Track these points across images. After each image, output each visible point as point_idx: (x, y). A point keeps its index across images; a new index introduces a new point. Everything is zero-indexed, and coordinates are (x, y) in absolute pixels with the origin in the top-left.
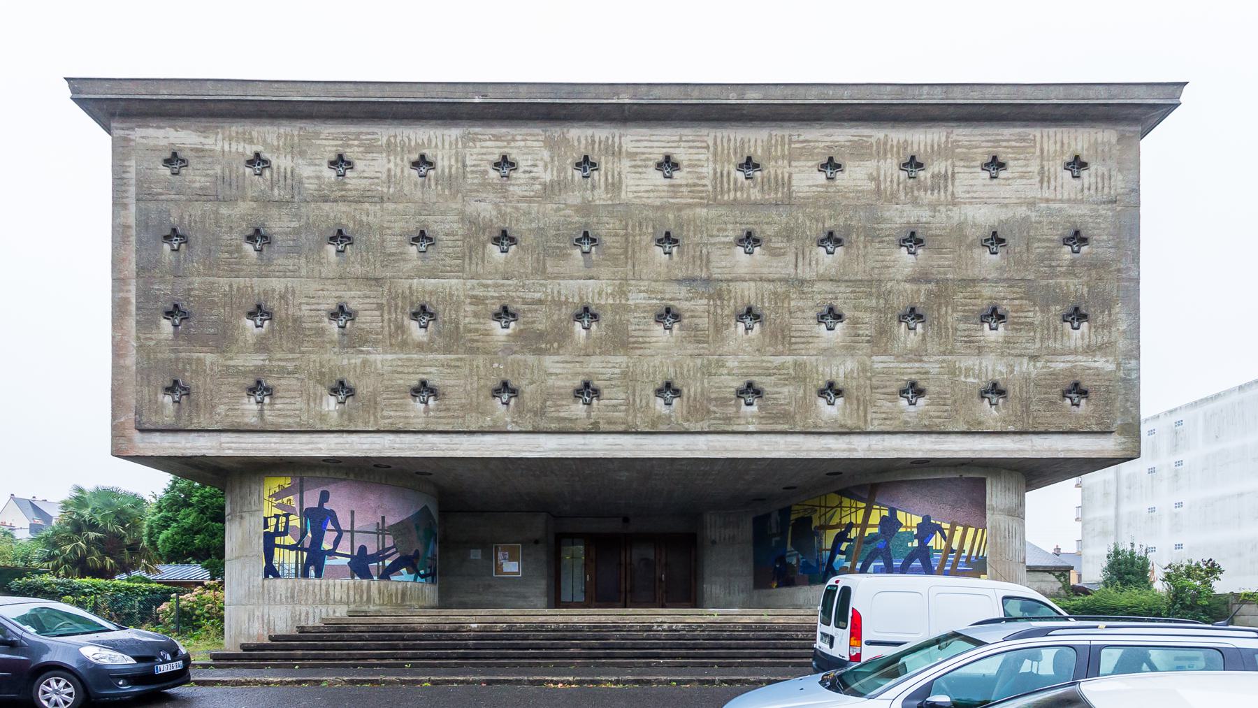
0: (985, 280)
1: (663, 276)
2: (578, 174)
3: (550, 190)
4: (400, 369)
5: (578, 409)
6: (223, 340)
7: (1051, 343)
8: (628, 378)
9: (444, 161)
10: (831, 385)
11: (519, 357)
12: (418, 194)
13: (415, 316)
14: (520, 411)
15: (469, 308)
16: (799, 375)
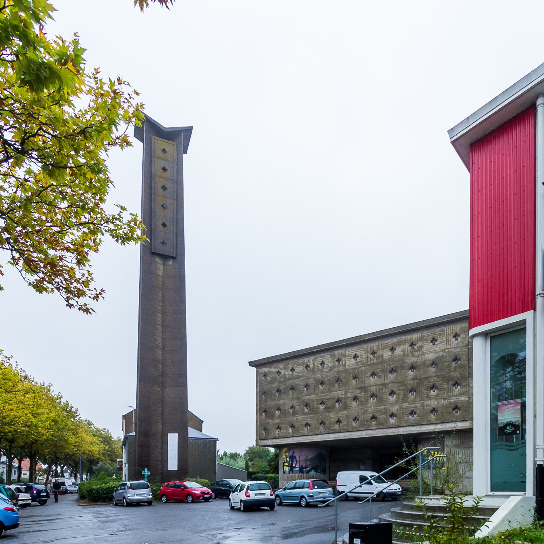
0: (431, 377)
1: (355, 388)
2: (337, 363)
3: (332, 368)
5: (337, 426)
6: (272, 417)
7: (449, 394)
8: (347, 417)
9: (311, 366)
14: (325, 428)
15: (316, 402)
16: (385, 411)
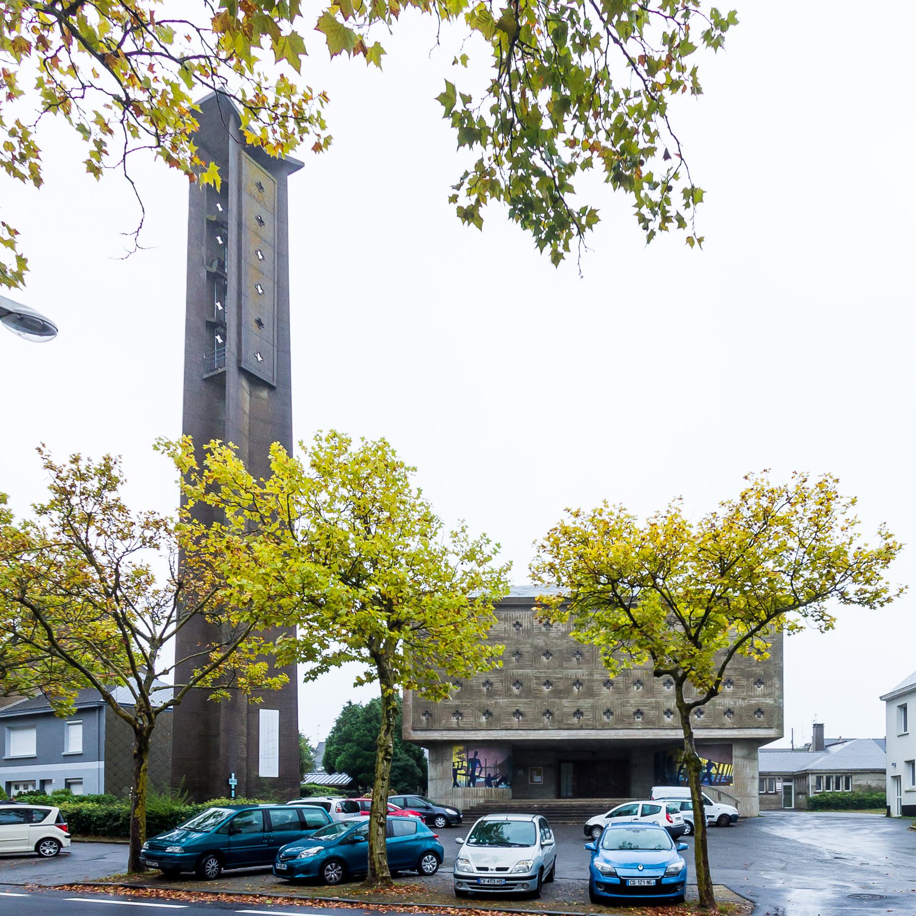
3: (565, 634)
5: (575, 720)
7: (750, 693)
8: (593, 708)
9: (525, 624)
10: (669, 710)
11: (553, 700)
12: (516, 637)
13: (514, 685)
14: (553, 721)
15: (534, 681)
16: (657, 706)
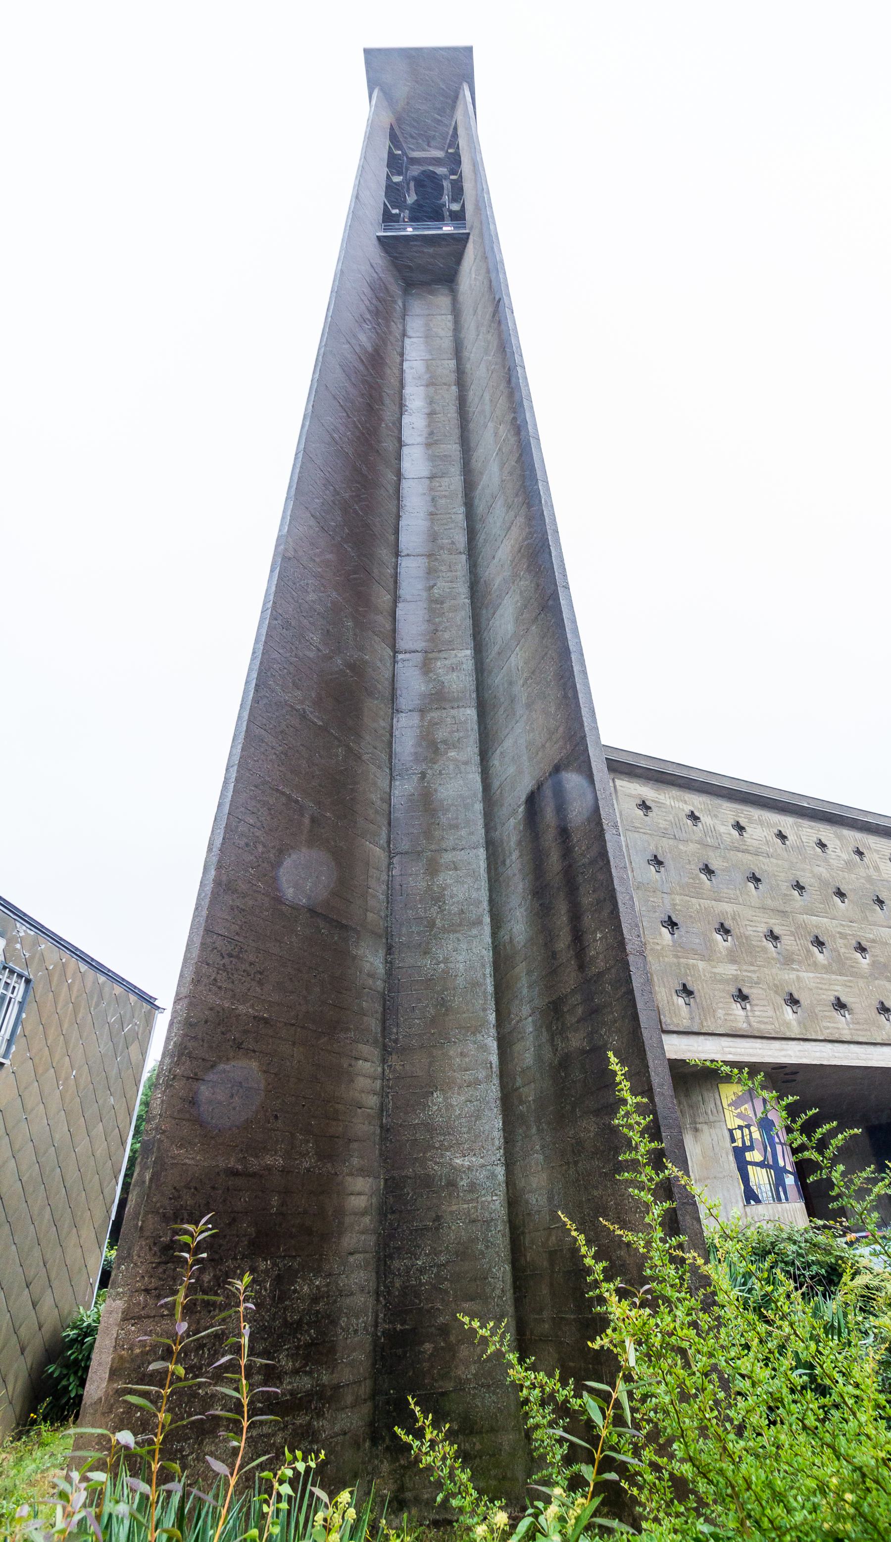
4: (820, 986)
